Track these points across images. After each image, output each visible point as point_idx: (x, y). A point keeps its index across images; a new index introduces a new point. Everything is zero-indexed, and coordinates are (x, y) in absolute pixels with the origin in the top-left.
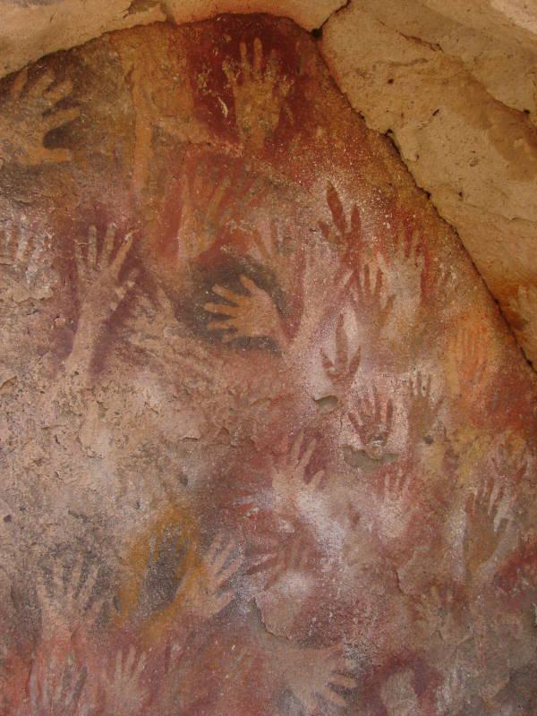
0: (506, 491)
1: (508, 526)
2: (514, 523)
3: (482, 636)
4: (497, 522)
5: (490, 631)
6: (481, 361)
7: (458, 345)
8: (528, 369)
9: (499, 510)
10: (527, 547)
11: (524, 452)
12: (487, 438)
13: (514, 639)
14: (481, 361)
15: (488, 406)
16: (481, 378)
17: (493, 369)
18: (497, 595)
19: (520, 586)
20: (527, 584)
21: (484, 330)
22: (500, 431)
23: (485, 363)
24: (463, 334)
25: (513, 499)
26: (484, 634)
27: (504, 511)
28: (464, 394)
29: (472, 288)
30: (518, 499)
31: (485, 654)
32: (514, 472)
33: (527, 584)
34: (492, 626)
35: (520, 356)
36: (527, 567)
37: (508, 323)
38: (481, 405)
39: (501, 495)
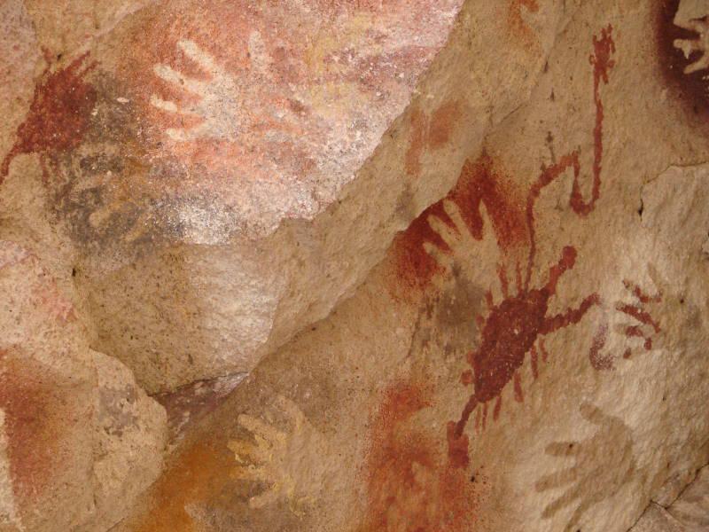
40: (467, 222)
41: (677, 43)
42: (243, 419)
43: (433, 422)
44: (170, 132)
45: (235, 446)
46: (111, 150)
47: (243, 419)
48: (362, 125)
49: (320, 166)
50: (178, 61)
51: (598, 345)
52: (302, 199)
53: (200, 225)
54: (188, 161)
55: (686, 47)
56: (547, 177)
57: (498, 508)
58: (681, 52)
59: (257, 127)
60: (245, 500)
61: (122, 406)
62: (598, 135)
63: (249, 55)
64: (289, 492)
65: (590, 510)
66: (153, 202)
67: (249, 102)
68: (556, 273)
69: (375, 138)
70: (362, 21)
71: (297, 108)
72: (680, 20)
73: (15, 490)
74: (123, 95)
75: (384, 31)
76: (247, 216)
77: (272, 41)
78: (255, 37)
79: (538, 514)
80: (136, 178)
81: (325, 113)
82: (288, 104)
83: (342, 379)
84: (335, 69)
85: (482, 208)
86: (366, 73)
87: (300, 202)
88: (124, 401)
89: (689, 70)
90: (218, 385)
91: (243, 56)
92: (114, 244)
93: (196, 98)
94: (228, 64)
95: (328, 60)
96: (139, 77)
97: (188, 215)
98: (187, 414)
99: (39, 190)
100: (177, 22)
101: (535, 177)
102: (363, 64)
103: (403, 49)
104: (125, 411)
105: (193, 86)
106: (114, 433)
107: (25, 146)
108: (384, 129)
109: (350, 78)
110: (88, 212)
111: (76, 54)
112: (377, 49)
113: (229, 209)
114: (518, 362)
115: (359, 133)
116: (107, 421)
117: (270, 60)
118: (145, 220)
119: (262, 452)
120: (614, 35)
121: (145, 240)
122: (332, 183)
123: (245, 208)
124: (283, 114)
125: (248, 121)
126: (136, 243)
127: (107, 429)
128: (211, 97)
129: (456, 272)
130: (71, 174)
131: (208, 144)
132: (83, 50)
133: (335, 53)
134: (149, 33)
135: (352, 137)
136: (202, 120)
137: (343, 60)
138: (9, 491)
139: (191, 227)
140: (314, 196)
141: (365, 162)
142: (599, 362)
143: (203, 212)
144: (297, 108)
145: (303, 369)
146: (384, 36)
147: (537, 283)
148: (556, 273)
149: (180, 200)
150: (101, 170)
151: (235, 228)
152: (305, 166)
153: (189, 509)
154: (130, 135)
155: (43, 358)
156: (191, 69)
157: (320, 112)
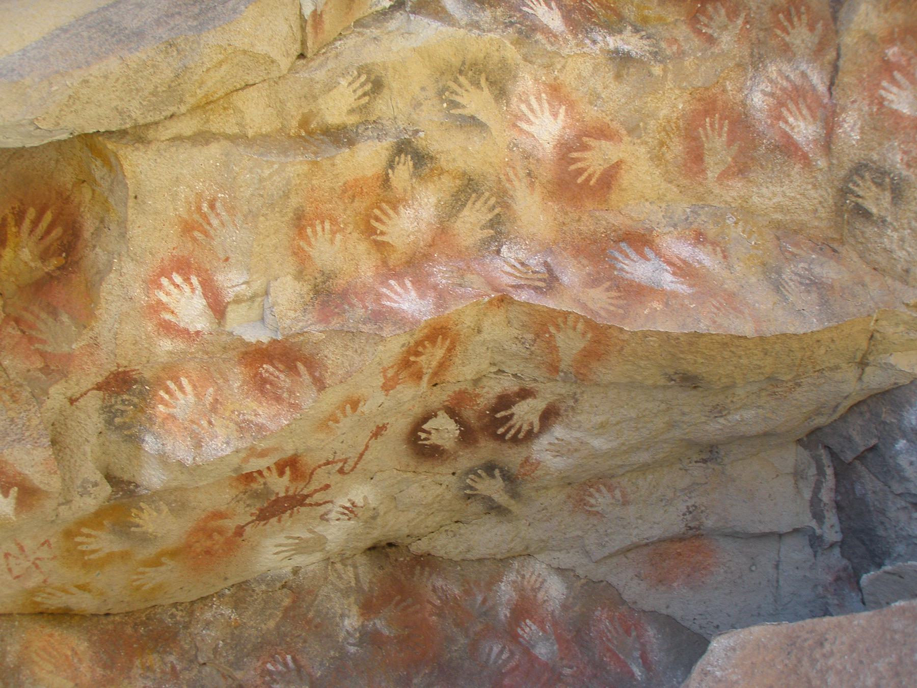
6: (69, 653)
7: (41, 663)
8: (111, 618)
11: (162, 659)
12: (126, 681)
14: (69, 653)
15: (105, 667)
16: (80, 660)
17: (83, 646)
21: (51, 635)
22: (130, 669)
23: (73, 650)
24: (38, 655)
28: (78, 681)
29: (14, 626)
32: (169, 676)
35: (96, 619)
37: (62, 616)
38: (99, 671)
41: (419, 433)
42: (142, 504)
43: (230, 524)
44: (160, 406)
45: (134, 511)
46: (136, 400)
47: (142, 504)
48: (228, 443)
51: (326, 514)
53: (150, 444)
54: (160, 420)
55: (423, 435)
56: (328, 463)
57: (253, 549)
59: (193, 422)
60: (130, 527)
62: (362, 455)
68: (316, 491)
69: (229, 451)
70: (254, 405)
71: (210, 423)
72: (425, 427)
73: (15, 509)
78: (211, 390)
80: (140, 414)
81: (221, 432)
85: (288, 469)
93: (177, 399)
95: (233, 412)
96: (159, 383)
97: (149, 438)
99: (100, 402)
102: (244, 421)
103: (263, 424)
105: (178, 394)
107: (99, 387)
109: (237, 423)
110: (116, 417)
111: (133, 368)
114: (284, 512)
116: (80, 490)
118: (134, 430)
119: (145, 515)
120: (388, 426)
121: (130, 436)
124: (204, 423)
128: (183, 402)
130: (116, 402)
131: (173, 417)
132: (137, 368)
134: (171, 370)
137: (240, 414)
140: (194, 459)
142: (323, 518)
144: (210, 423)
145: (176, 496)
147: (305, 492)
148: (316, 491)
149: (148, 431)
150: (129, 405)
152: (198, 445)
153: (105, 522)
154: (145, 399)
155: (35, 481)
156: (181, 388)
157: (217, 429)
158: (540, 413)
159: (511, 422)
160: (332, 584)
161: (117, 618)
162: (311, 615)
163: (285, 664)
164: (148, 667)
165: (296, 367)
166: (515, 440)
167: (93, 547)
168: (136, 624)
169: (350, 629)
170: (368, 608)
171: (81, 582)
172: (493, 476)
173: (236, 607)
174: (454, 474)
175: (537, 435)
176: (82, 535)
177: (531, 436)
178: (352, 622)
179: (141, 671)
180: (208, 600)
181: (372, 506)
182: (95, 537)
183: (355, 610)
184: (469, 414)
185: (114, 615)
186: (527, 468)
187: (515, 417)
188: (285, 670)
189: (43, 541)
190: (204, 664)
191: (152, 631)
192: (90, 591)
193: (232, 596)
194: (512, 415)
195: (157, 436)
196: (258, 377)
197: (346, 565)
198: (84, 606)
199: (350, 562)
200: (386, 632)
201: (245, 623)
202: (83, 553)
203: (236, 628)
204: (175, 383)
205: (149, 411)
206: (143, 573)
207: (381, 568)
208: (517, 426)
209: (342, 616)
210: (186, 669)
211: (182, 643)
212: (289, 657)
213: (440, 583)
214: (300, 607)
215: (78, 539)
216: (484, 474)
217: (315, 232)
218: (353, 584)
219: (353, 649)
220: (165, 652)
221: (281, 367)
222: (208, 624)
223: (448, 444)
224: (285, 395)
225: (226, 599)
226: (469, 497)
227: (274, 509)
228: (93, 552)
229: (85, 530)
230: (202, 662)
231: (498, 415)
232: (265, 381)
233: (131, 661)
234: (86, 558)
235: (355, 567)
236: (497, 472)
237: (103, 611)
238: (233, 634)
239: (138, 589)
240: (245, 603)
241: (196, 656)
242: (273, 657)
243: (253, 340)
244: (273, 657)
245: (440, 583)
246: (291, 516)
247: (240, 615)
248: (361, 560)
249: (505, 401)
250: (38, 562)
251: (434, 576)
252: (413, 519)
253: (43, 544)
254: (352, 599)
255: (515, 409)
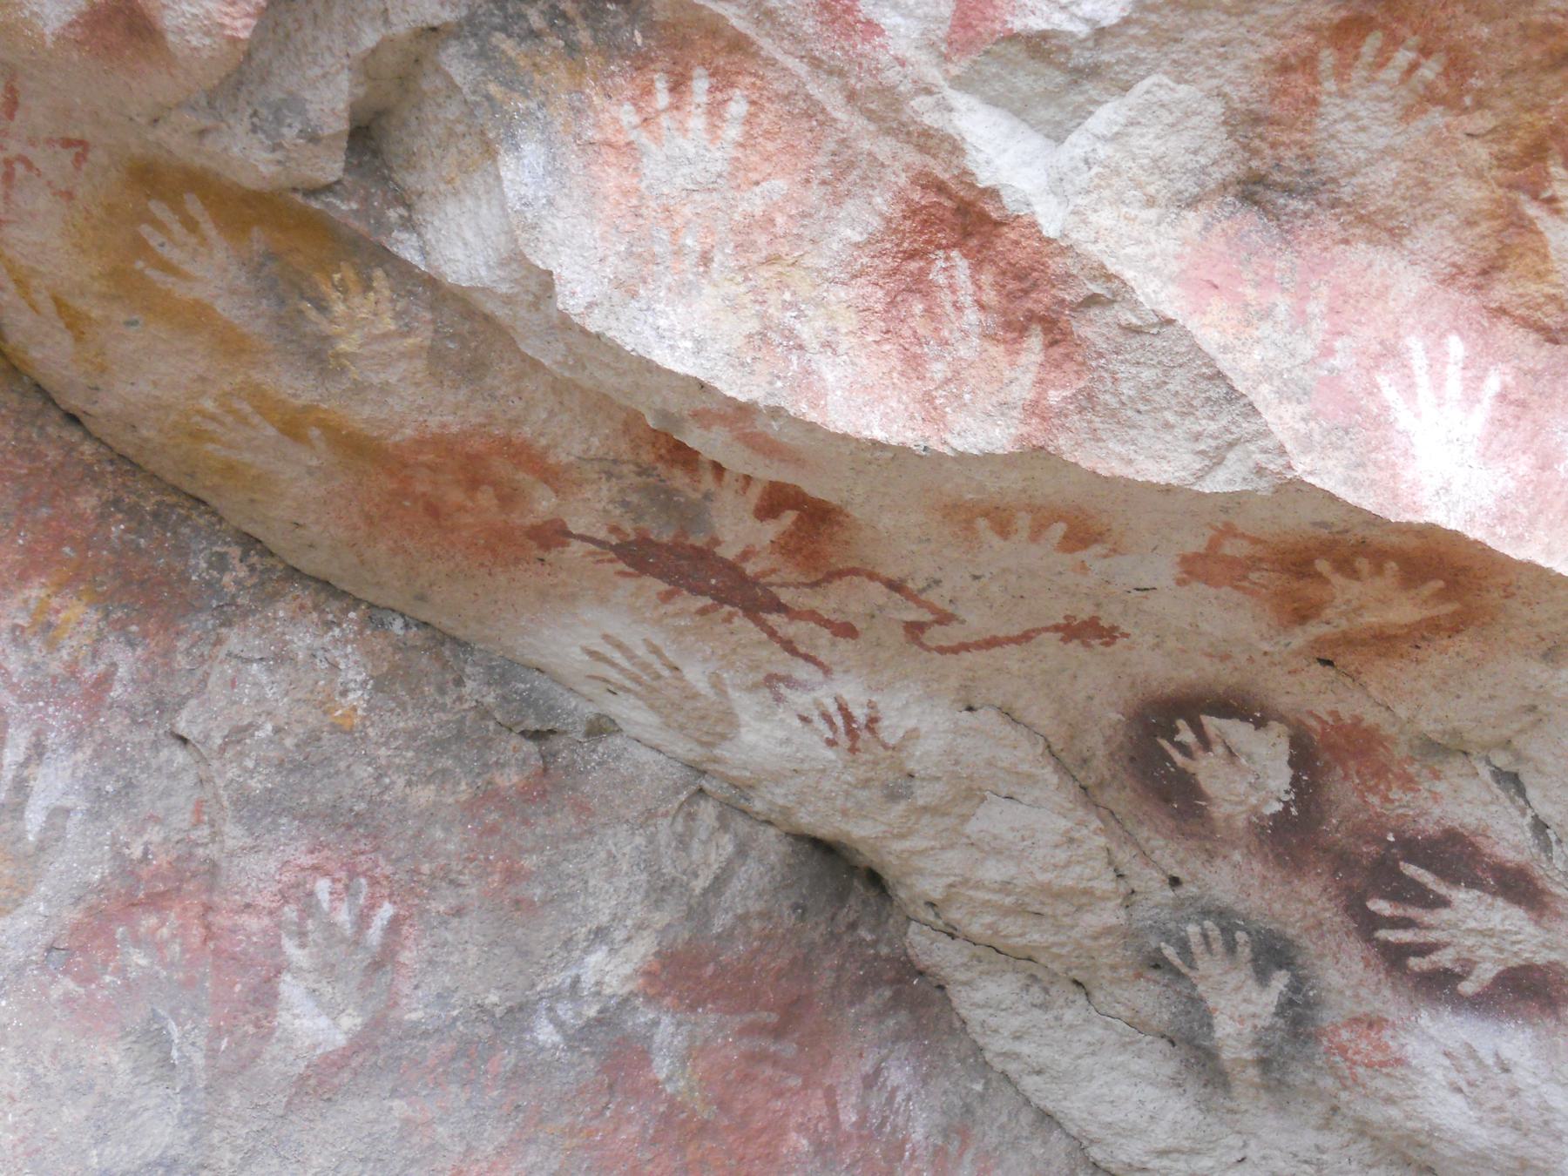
0: (51, 738)
1: (73, 824)
2: (95, 815)
3: (13, 1099)
4: (34, 820)
5: (35, 1082)
8: (74, 435)
9: (37, 785)
10: (144, 872)
11: (101, 638)
13: (104, 1098)
18: (56, 993)
19: (121, 971)
20: (143, 962)
25: (80, 756)
26: (17, 1092)
27: (54, 784)
30: (97, 755)
31: (22, 1140)
33: (143, 962)
34: (40, 1070)
35: (36, 404)
36: (151, 921)
39: (38, 751)
40: (762, 499)
41: (1181, 724)
44: (628, 107)
48: (700, 346)
49: (634, 304)
50: (719, 96)
51: (789, 681)
52: (583, 290)
56: (895, 586)
57: (543, 596)
58: (1177, 731)
61: (290, 126)
63: (757, 183)
64: (343, 346)
65: (640, 703)
66: (541, 105)
67: (697, 197)
68: (813, 616)
70: (847, 322)
71: (705, 259)
72: (1211, 723)
73: (71, 25)
74: (645, 37)
75: (841, 349)
76: (547, 227)
77: (781, 209)
79: (584, 642)
81: (708, 300)
82: (707, 247)
83: (496, 383)
84: (773, 297)
85: (789, 517)
86: (775, 337)
87: (578, 289)
88: (297, 126)
89: (1165, 743)
90: (404, 236)
91: (754, 176)
92: (480, 70)
94: (737, 159)
97: (532, 151)
98: (354, 206)
100: (758, 82)
101: (892, 572)
102: (789, 334)
104: (285, 130)
105: (697, 122)
106: (253, 124)
108: (702, 377)
112: (814, 345)
113: (551, 203)
114: (696, 591)
115: (689, 344)
116: (264, 112)
117: (758, 212)
120: (1121, 642)
122: (614, 324)
123: (556, 226)
125: (672, 202)
126: (489, 98)
127: (255, 114)
129: (707, 496)
133: (794, 293)
135: (683, 335)
136: (657, 140)
138: (67, 18)
139: (519, 158)
140: (591, 305)
141: (649, 361)
143: (540, 171)
146: (835, 352)
147: (785, 596)
148: (813, 616)
149: (548, 142)
151: (529, 215)
158: (1514, 962)
159: (1427, 917)
160: (651, 840)
161: (87, 448)
162: (530, 862)
163: (363, 920)
164: (49, 625)
165: (1023, 330)
166: (1395, 957)
167: (174, 255)
168: (116, 502)
169: (588, 980)
170: (680, 974)
171: (79, 304)
172: (1262, 977)
173: (381, 684)
174: (1175, 882)
175: (1461, 1003)
176: (177, 207)
177: (1439, 986)
178: (609, 970)
179: (22, 620)
180: (335, 605)
181: (911, 766)
182: (204, 240)
183: (643, 949)
184: (1345, 793)
185: (88, 434)
186: (1363, 1045)
187: (1445, 914)
188: (348, 930)
189: (75, 134)
190: (184, 741)
191: (138, 549)
192: (79, 338)
193: (400, 647)
194: (1444, 902)
195: (555, 168)
196: (914, 266)
197: (724, 826)
198: (36, 354)
199: (741, 825)
200: (662, 1067)
201: (365, 738)
202: (141, 247)
203: (335, 728)
204: (712, 90)
205: (591, 90)
206: (243, 420)
207: (801, 909)
208: (1432, 937)
209: (600, 935)
210: (129, 709)
211: (182, 644)
212: (386, 911)
213: (897, 1076)
214: (525, 822)
215: (158, 209)
216: (1245, 952)
217: (1382, 62)
218: (699, 885)
219: (546, 1033)
220: (121, 627)
221: (990, 296)
222: (280, 658)
223: (1226, 809)
224: (938, 370)
225: (378, 643)
226: (1157, 963)
227: (673, 560)
228: (168, 267)
229: (194, 205)
230: (182, 727)
231: (1411, 870)
232: (920, 286)
233: (23, 578)
234: (140, 265)
235: (742, 851)
236: (1280, 980)
237: (75, 402)
238: (314, 737)
239: (197, 435)
240: (411, 692)
241: (182, 702)
242: (353, 874)
243: (985, 179)
244: (353, 874)
245: (897, 1076)
246: (703, 612)
247: (370, 709)
248: (771, 844)
249: (1457, 856)
250: (20, 169)
251: (903, 1048)
252: (979, 885)
253: (68, 143)
254: (660, 918)
255: (1461, 896)
